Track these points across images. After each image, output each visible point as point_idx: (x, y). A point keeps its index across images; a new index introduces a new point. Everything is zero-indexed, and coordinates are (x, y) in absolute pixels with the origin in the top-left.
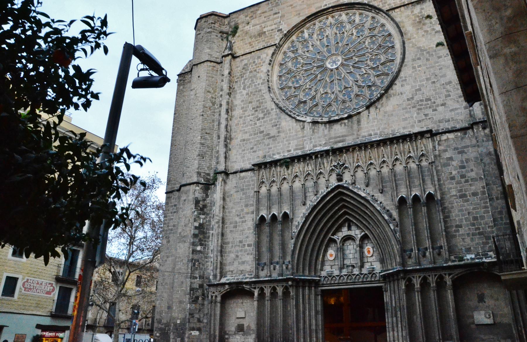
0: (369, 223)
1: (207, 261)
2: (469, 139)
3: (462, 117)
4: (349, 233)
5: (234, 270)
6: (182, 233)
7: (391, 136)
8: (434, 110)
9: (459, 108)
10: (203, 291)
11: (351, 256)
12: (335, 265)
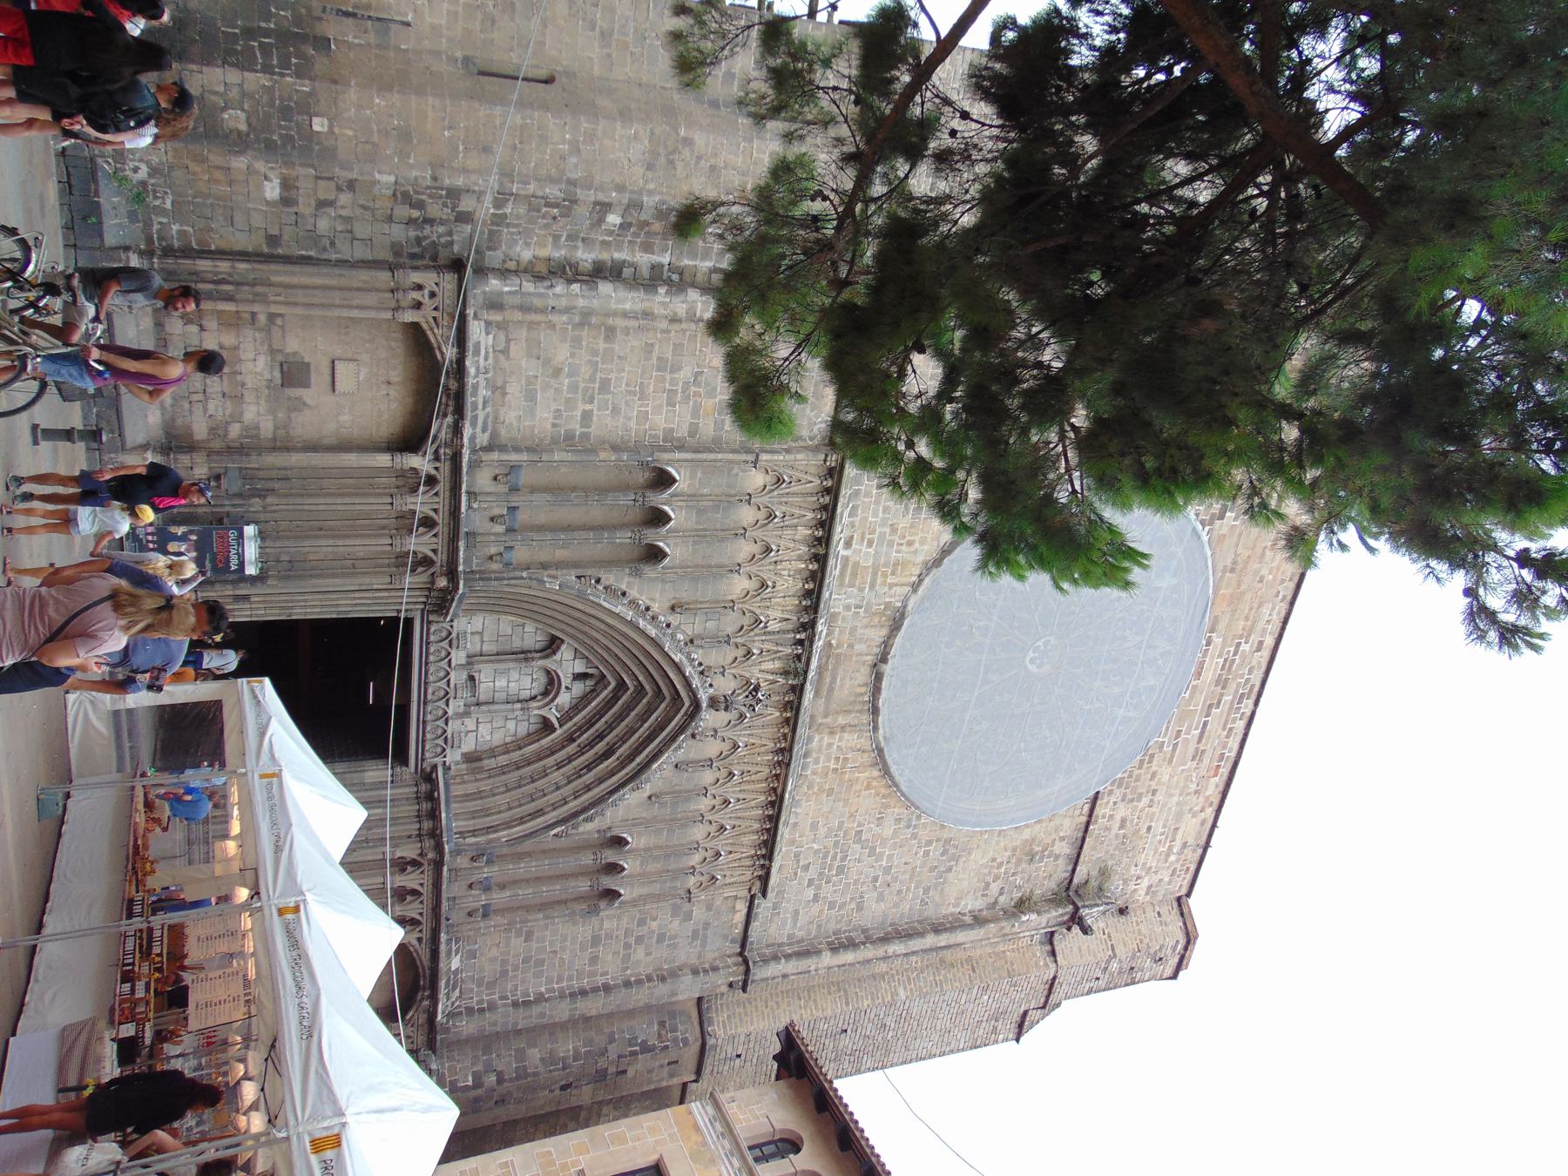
0: (581, 752)
1: (559, 237)
2: (720, 946)
3: (773, 929)
4: (566, 681)
5: (508, 358)
6: (686, 153)
7: (783, 819)
8: (811, 882)
9: (795, 924)
10: (443, 221)
11: (501, 683)
12: (482, 642)
